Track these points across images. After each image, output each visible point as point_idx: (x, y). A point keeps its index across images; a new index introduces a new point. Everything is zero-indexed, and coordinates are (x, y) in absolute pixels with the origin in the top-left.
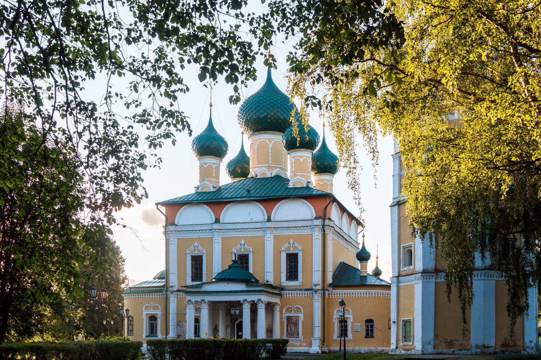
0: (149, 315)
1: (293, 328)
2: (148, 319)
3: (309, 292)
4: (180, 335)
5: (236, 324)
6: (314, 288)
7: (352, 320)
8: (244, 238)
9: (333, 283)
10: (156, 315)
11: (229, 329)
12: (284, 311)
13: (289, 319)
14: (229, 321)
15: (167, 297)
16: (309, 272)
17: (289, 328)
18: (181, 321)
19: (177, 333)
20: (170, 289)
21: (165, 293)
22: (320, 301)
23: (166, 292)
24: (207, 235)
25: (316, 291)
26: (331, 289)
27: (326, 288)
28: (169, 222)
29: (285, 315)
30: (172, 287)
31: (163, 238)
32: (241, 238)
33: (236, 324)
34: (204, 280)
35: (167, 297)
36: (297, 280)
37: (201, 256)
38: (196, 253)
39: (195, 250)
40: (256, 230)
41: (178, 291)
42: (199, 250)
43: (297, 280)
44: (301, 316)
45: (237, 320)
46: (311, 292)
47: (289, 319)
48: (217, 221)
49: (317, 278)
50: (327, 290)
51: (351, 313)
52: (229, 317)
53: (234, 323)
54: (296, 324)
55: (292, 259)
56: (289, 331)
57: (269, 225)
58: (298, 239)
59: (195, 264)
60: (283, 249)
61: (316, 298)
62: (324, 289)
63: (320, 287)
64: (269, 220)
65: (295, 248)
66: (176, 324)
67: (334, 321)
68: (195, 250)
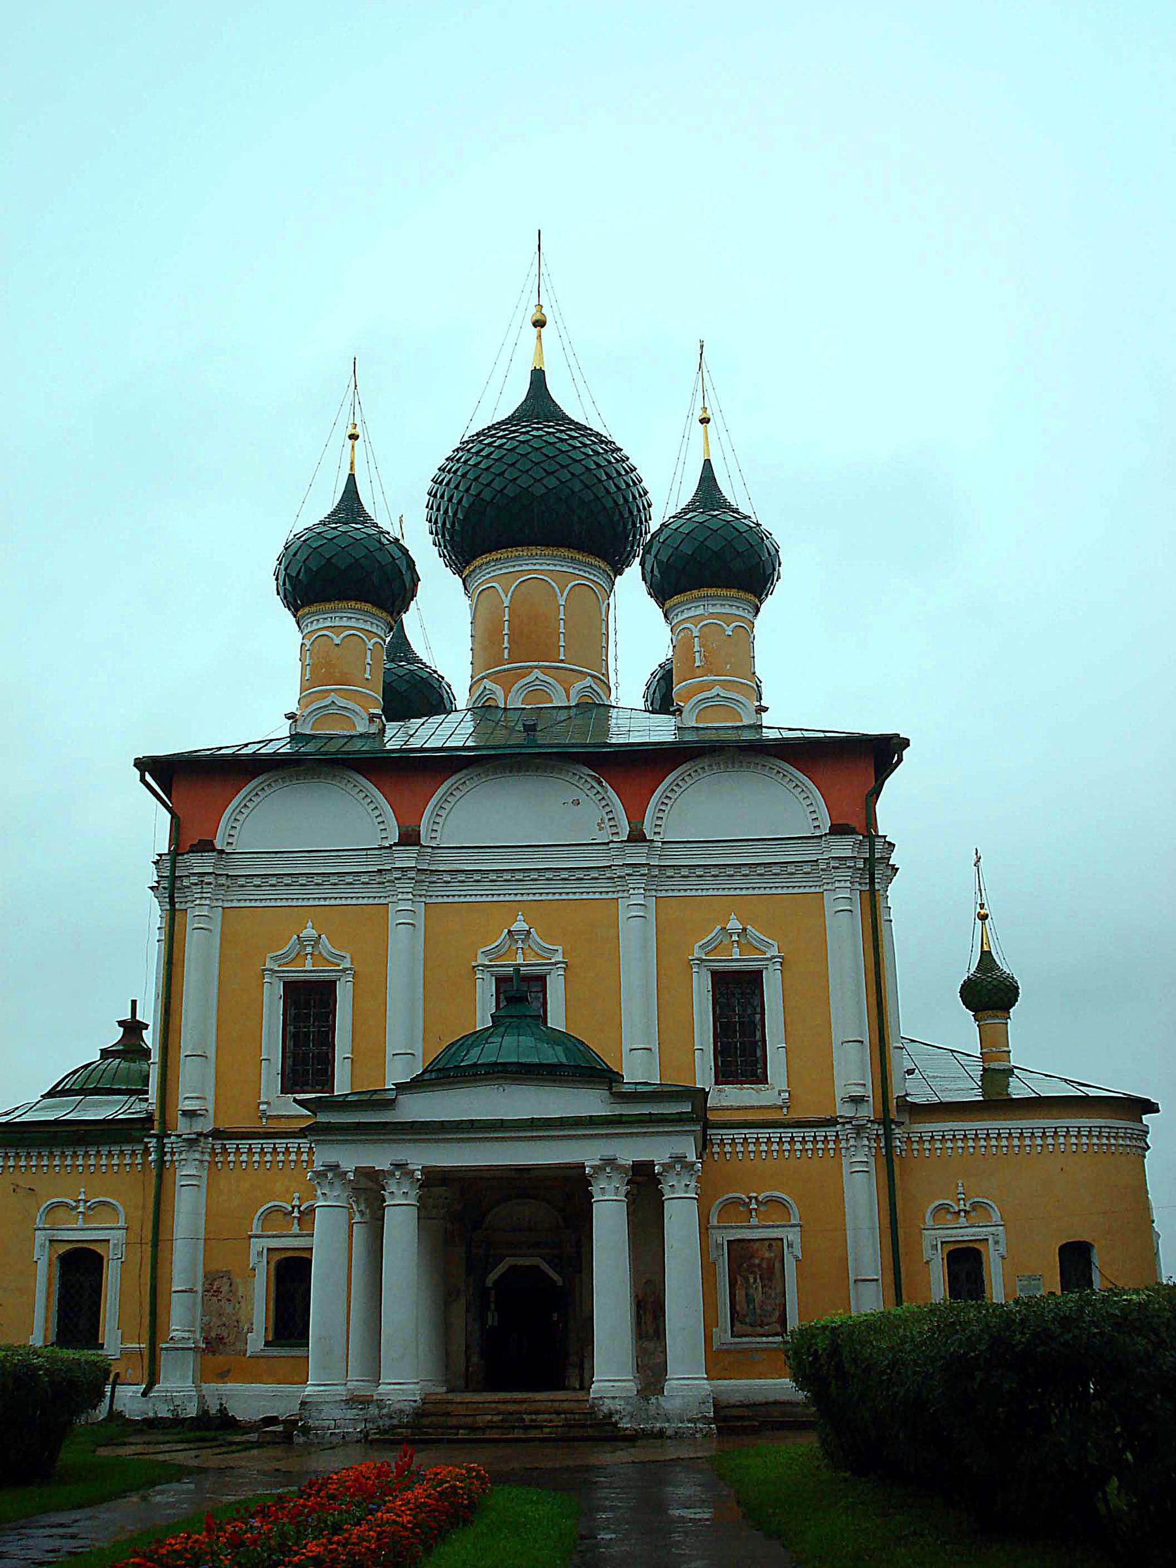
0: (62, 1249)
1: (759, 1297)
2: (57, 1263)
3: (821, 1133)
4: (220, 1339)
7: (1002, 1249)
10: (99, 1248)
12: (714, 1221)
13: (740, 1252)
15: (161, 1162)
17: (740, 1294)
18: (227, 1275)
19: (207, 1328)
20: (183, 1126)
21: (153, 1143)
23: (160, 1138)
25: (859, 1130)
26: (906, 1119)
27: (893, 1114)
28: (192, 837)
29: (722, 1237)
30: (190, 1114)
31: (152, 912)
34: (342, 1085)
35: (161, 1162)
37: (329, 987)
41: (217, 1134)
42: (317, 957)
44: (792, 1235)
46: (831, 1132)
47: (740, 1252)
50: (900, 1124)
51: (996, 1216)
54: (772, 1273)
59: (296, 1018)
62: (886, 1122)
63: (867, 1112)
66: (199, 1288)
67: (927, 1254)
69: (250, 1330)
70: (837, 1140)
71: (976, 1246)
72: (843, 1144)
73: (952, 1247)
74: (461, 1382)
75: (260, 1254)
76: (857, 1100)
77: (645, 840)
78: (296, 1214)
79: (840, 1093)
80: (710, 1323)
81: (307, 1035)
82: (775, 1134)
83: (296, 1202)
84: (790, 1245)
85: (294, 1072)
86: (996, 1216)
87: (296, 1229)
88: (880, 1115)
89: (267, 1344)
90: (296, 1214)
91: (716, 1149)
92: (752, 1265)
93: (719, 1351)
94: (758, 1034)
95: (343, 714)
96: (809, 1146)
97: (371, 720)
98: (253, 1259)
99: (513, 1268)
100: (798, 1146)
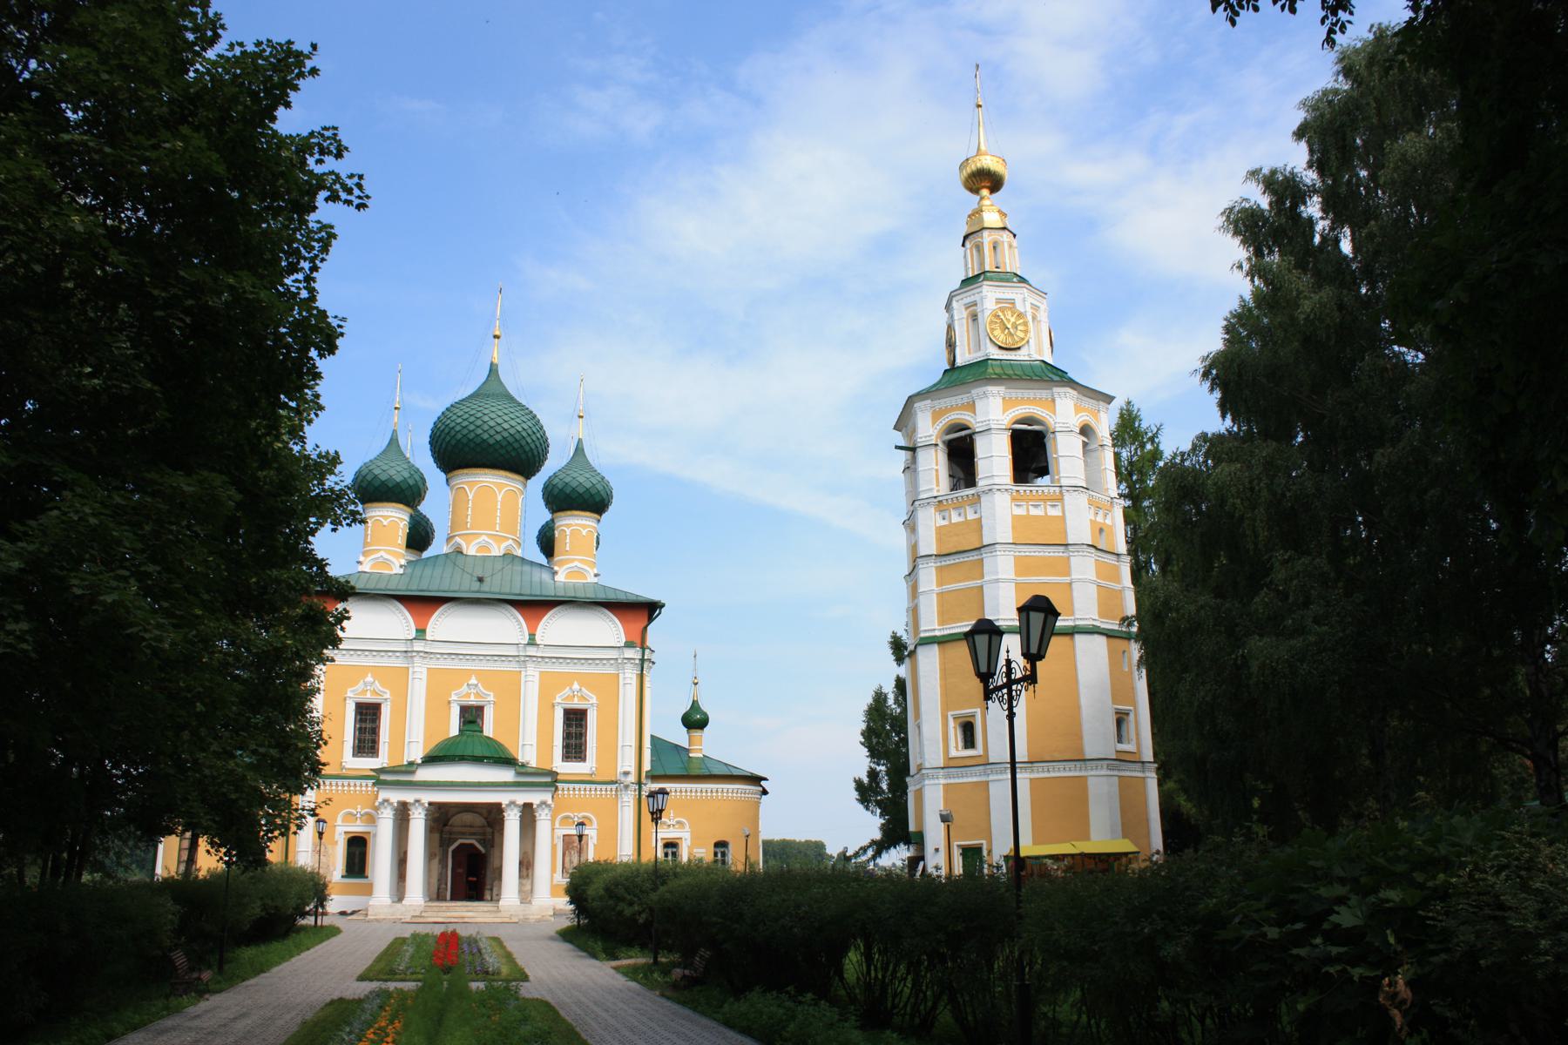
3: (609, 787)
5: (451, 849)
6: (623, 779)
7: (689, 842)
8: (478, 673)
9: (651, 770)
11: (436, 861)
12: (557, 825)
14: (437, 843)
16: (610, 749)
17: (567, 859)
22: (632, 804)
24: (399, 662)
25: (627, 787)
26: (649, 781)
29: (561, 832)
32: (469, 673)
33: (451, 849)
36: (584, 759)
38: (369, 698)
39: (364, 692)
40: (503, 659)
43: (584, 759)
45: (456, 840)
46: (614, 787)
48: (421, 632)
49: (627, 762)
52: (437, 836)
53: (448, 846)
55: (575, 719)
56: (567, 865)
57: (532, 651)
58: (585, 680)
60: (558, 700)
61: (626, 799)
62: (640, 783)
63: (632, 778)
64: (532, 642)
65: (583, 698)
66: (310, 850)
68: (364, 692)
69: (335, 870)
70: (616, 790)
71: (677, 841)
72: (619, 793)
73: (666, 841)
74: (435, 896)
75: (340, 834)
76: (626, 774)
77: (536, 645)
78: (358, 815)
79: (620, 770)
80: (553, 870)
81: (366, 728)
82: (588, 786)
83: (359, 810)
84: (591, 838)
85: (359, 747)
86: (687, 828)
87: (358, 822)
88: (637, 779)
89: (342, 877)
90: (358, 815)
91: (560, 792)
92: (573, 847)
93: (555, 885)
94: (583, 739)
95: (387, 563)
96: (604, 792)
97: (401, 566)
98: (337, 837)
99: (461, 845)
100: (598, 793)
